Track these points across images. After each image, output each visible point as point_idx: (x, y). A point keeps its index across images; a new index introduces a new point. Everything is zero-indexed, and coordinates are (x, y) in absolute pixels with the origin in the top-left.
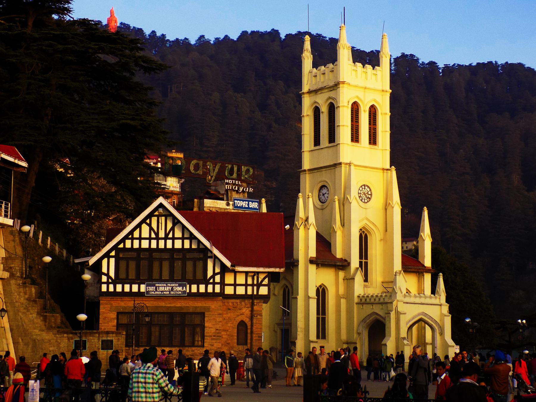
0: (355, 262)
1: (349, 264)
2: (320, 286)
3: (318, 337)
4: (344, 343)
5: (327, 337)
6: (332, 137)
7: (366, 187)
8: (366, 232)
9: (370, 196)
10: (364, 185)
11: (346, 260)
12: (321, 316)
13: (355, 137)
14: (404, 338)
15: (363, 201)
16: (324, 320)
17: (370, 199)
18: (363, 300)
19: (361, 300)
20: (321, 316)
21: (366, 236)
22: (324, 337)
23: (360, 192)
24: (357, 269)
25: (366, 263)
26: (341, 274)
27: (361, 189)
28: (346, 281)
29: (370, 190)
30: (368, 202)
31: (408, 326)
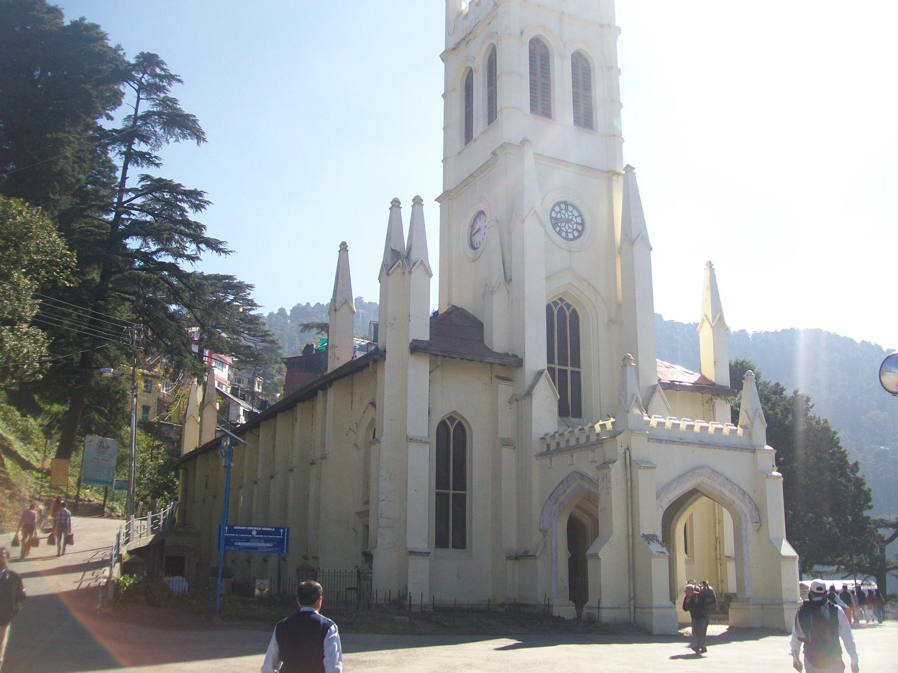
0: (536, 357)
1: (520, 363)
2: (452, 419)
3: (441, 541)
4: (508, 558)
5: (468, 545)
7: (570, 208)
8: (574, 306)
9: (580, 228)
10: (565, 203)
11: (514, 356)
12: (451, 492)
13: (541, 101)
14: (650, 538)
15: (564, 234)
16: (461, 502)
17: (581, 233)
18: (553, 447)
19: (548, 446)
20: (451, 492)
21: (574, 314)
22: (461, 543)
23: (554, 215)
24: (540, 373)
25: (577, 376)
26: (504, 390)
27: (557, 209)
28: (515, 404)
29: (580, 215)
30: (575, 238)
31: (666, 503)
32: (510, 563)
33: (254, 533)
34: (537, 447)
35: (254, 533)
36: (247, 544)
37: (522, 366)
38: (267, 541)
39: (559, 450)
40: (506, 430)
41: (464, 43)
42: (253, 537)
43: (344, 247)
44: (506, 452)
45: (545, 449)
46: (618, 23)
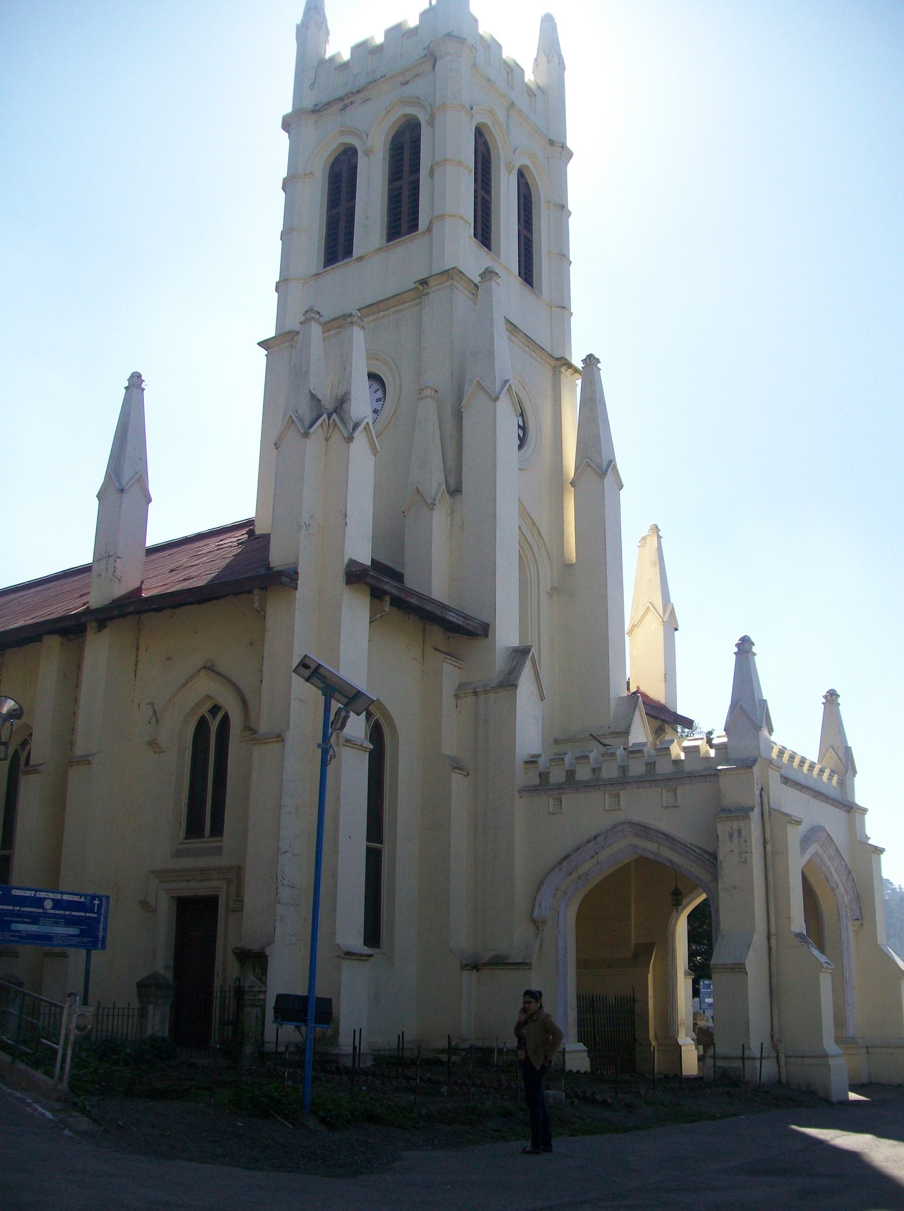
6: (403, 218)
32: (466, 974)
33: (48, 904)
34: (522, 777)
35: (48, 904)
36: (33, 928)
37: (486, 635)
38: (71, 922)
39: (571, 782)
40: (450, 745)
41: (340, 106)
42: (46, 915)
43: (135, 383)
44: (456, 778)
45: (536, 781)
46: (571, 144)
